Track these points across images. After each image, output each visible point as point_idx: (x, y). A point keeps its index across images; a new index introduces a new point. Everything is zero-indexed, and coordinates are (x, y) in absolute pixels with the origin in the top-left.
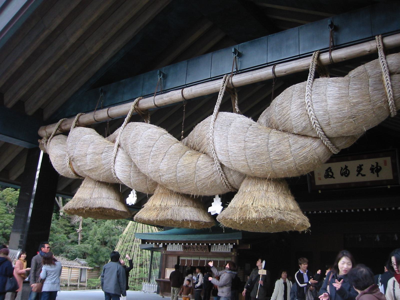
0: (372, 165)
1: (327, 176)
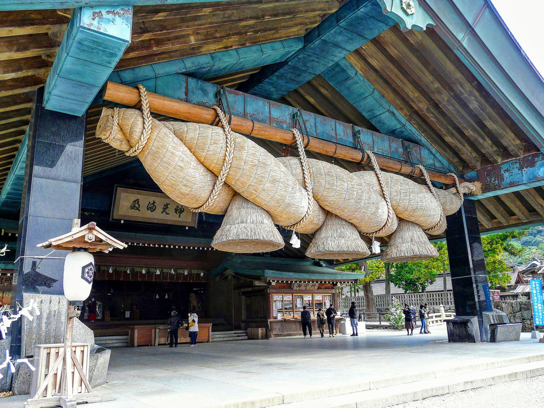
1: (133, 207)
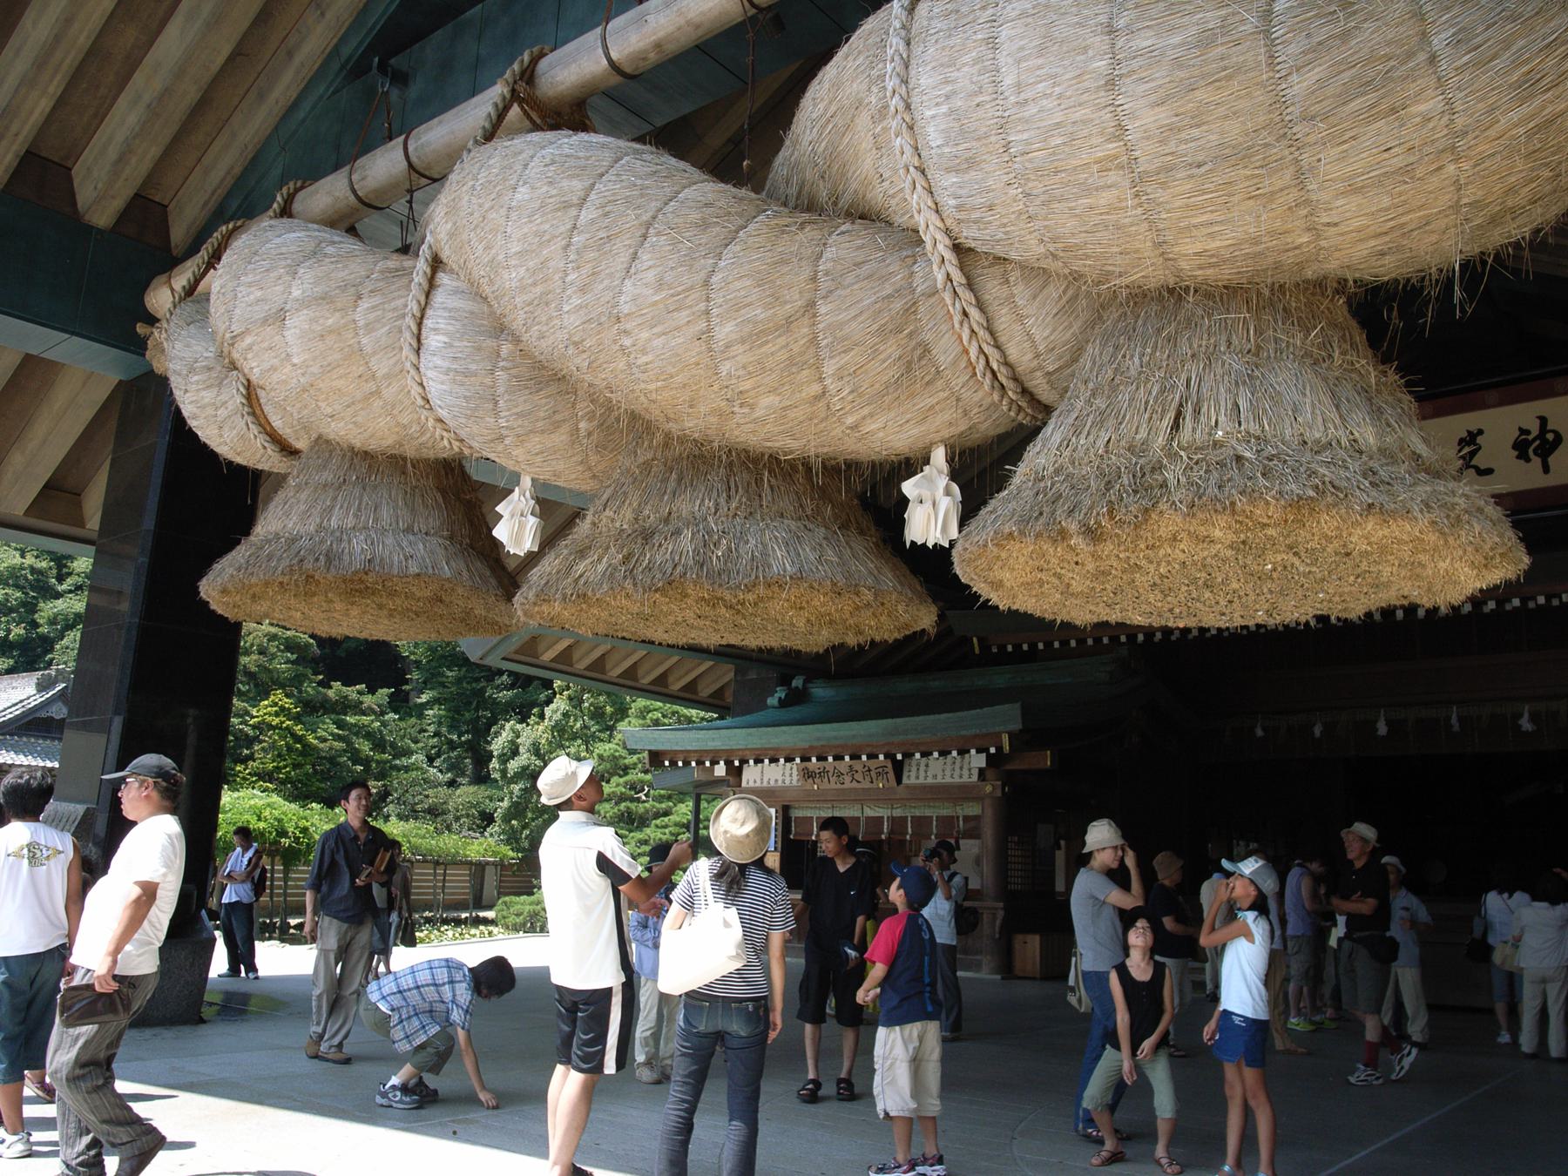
0: (1520, 429)
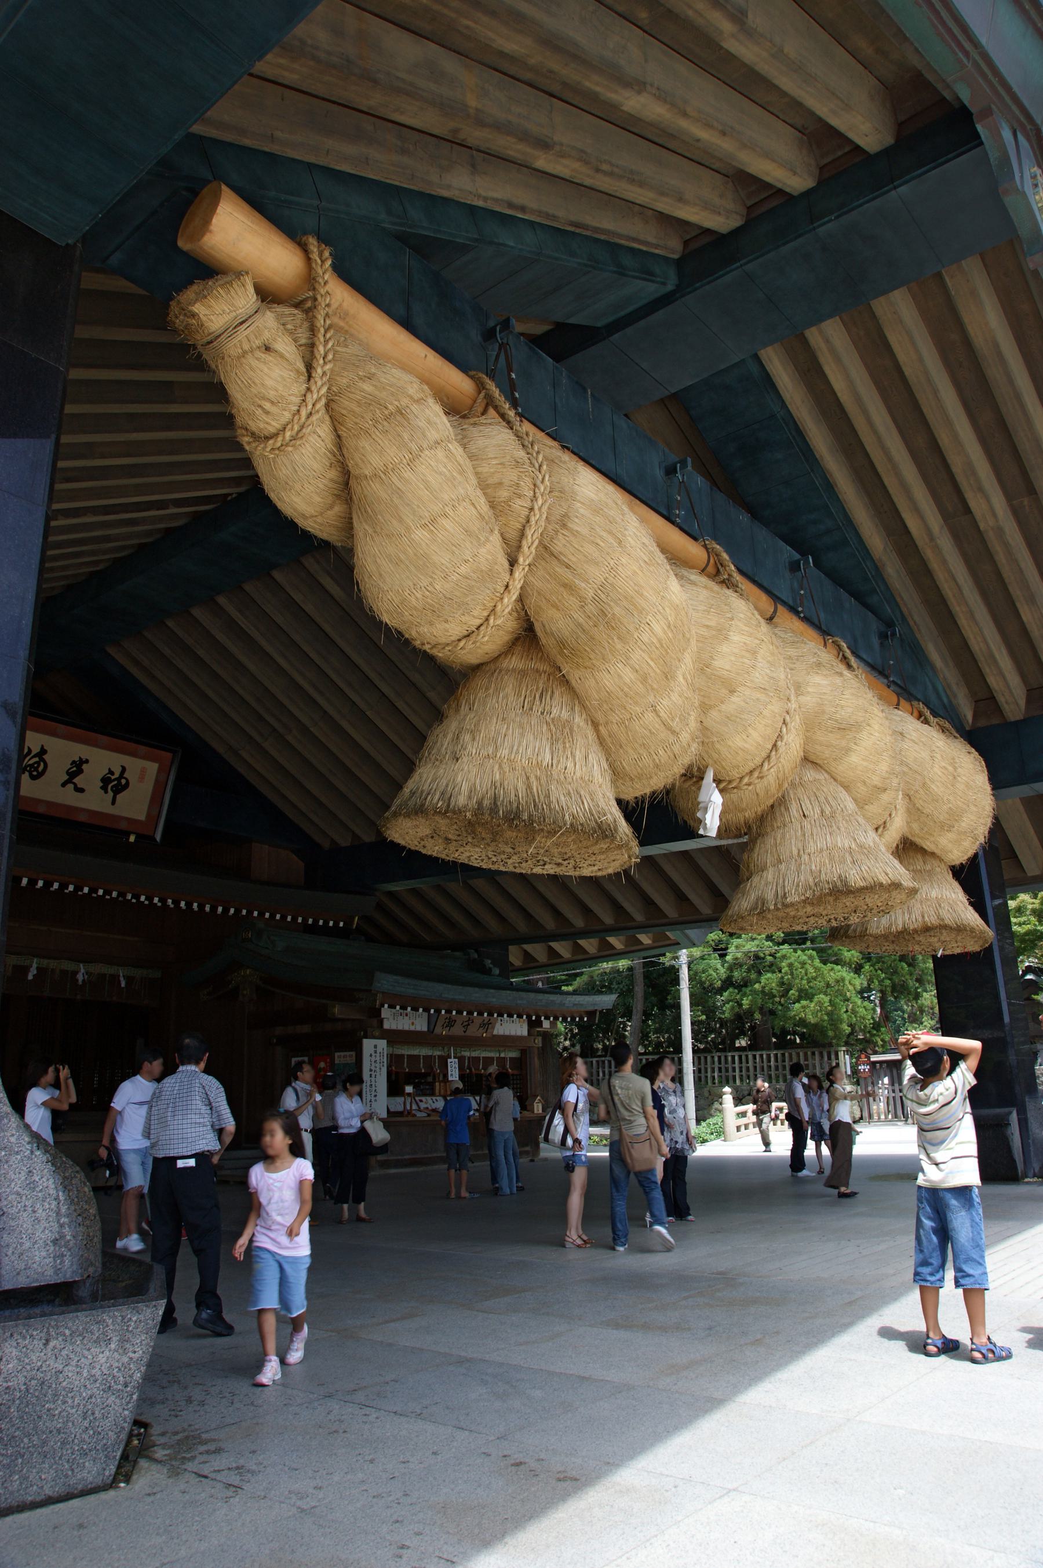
0: (109, 769)
